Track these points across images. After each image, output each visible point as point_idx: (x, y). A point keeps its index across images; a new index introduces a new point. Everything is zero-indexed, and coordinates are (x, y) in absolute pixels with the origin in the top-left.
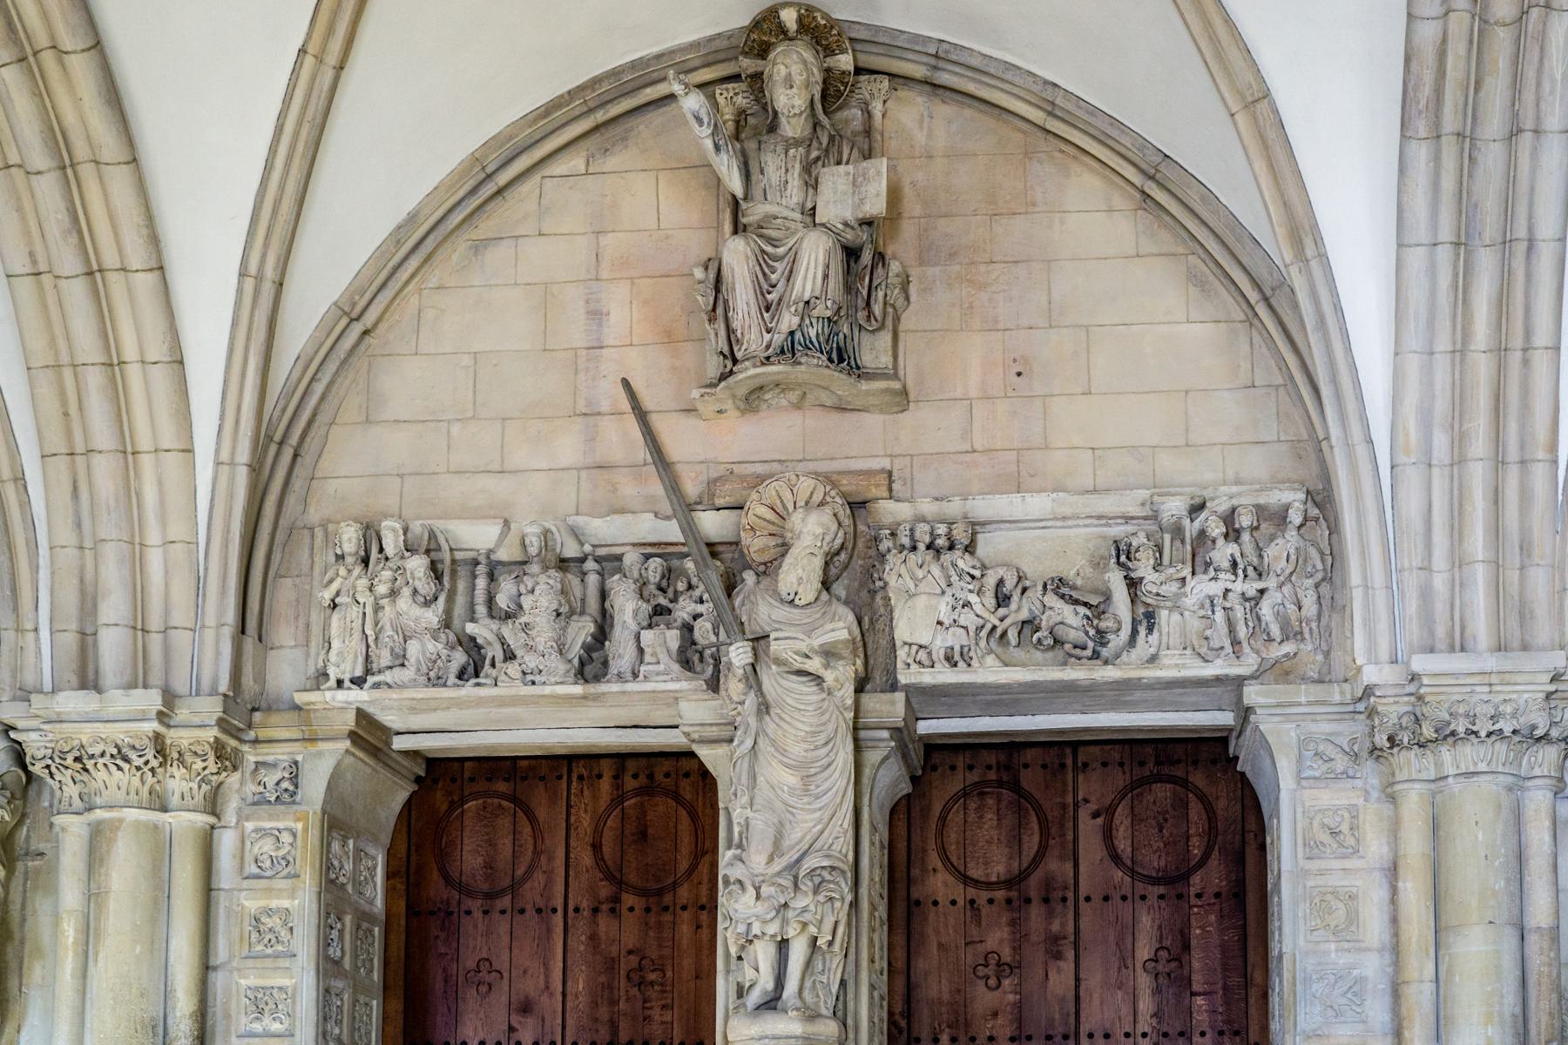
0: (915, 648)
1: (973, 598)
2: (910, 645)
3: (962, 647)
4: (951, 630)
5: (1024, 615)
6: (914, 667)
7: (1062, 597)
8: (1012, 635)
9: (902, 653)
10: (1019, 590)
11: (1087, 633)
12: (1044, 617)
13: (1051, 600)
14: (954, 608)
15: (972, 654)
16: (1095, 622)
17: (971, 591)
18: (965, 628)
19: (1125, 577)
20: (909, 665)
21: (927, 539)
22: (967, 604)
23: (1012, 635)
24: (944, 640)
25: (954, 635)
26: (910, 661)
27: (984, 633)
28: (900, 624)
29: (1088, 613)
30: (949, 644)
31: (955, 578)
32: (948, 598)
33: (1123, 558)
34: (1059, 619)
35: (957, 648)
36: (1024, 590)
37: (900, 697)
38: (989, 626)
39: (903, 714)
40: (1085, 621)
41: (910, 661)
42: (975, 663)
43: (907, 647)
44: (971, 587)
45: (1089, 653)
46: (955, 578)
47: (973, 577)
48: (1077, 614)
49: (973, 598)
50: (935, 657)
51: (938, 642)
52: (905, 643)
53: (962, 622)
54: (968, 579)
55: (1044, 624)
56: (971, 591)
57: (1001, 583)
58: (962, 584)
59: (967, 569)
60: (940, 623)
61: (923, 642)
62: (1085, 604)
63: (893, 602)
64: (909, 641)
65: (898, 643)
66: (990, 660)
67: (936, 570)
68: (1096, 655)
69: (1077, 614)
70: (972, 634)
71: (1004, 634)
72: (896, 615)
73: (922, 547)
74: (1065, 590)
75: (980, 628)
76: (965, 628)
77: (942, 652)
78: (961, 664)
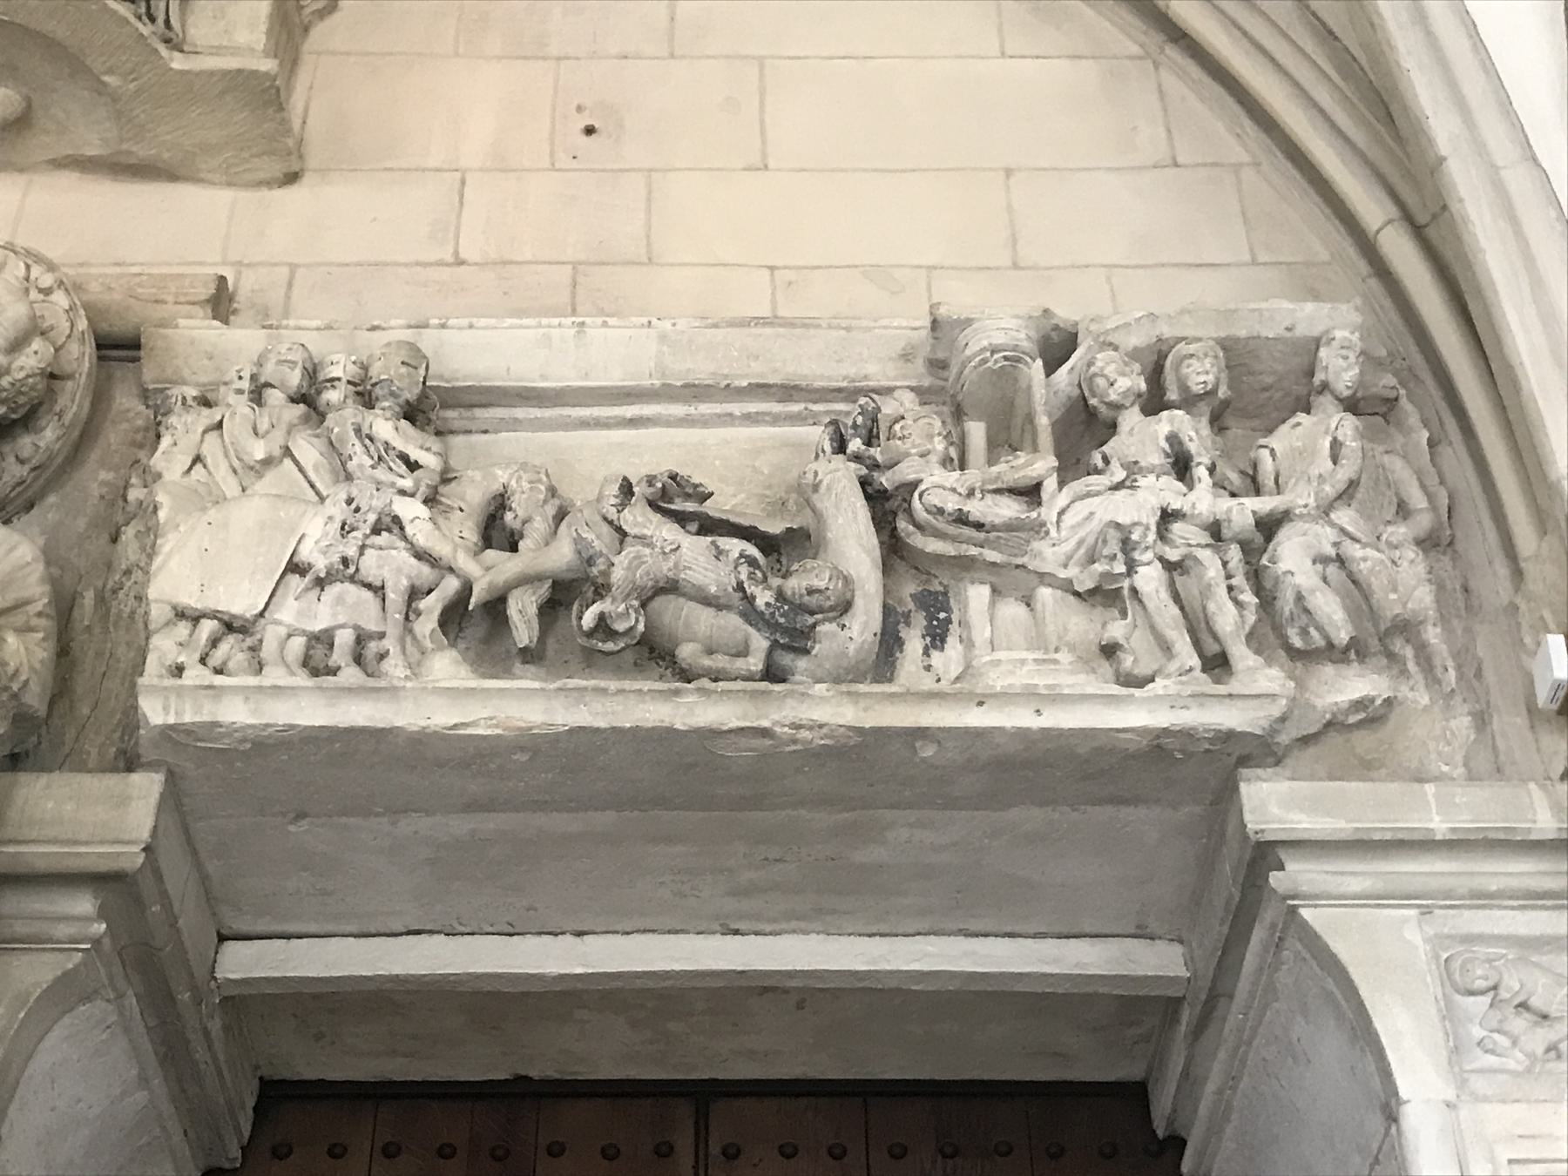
0: (208, 627)
1: (411, 511)
2: (196, 618)
3: (361, 639)
4: (334, 590)
5: (560, 556)
6: (195, 675)
7: (681, 519)
8: (523, 611)
9: (165, 647)
10: (551, 510)
11: (750, 613)
12: (621, 561)
13: (638, 518)
14: (345, 529)
15: (389, 644)
16: (775, 582)
17: (402, 492)
18: (378, 590)
19: (864, 483)
20: (179, 670)
21: (295, 378)
22: (390, 524)
23: (523, 611)
24: (300, 614)
25: (340, 600)
26: (188, 658)
27: (432, 605)
28: (173, 564)
29: (753, 551)
30: (318, 626)
31: (360, 459)
32: (337, 509)
33: (855, 445)
34: (665, 568)
35: (344, 638)
36: (561, 516)
37: (146, 787)
38: (451, 585)
39: (145, 835)
40: (744, 571)
41: (188, 658)
42: (395, 668)
43: (183, 629)
44: (407, 483)
45: (755, 663)
46: (360, 459)
47: (413, 466)
48: (719, 553)
49: (411, 511)
50: (269, 650)
51: (288, 612)
52: (181, 614)
53: (371, 565)
54: (403, 469)
55: (617, 575)
56: (402, 492)
57: (500, 504)
58: (381, 474)
59: (399, 444)
60: (295, 567)
61: (243, 604)
62: (747, 533)
63: (162, 514)
64: (193, 601)
65: (158, 613)
66: (447, 667)
67: (308, 450)
68: (773, 674)
69: (719, 553)
70: (395, 597)
71: (496, 607)
72: (166, 545)
73: (275, 397)
74: (679, 505)
75: (415, 594)
76: (378, 590)
77: (298, 644)
78: (351, 674)
